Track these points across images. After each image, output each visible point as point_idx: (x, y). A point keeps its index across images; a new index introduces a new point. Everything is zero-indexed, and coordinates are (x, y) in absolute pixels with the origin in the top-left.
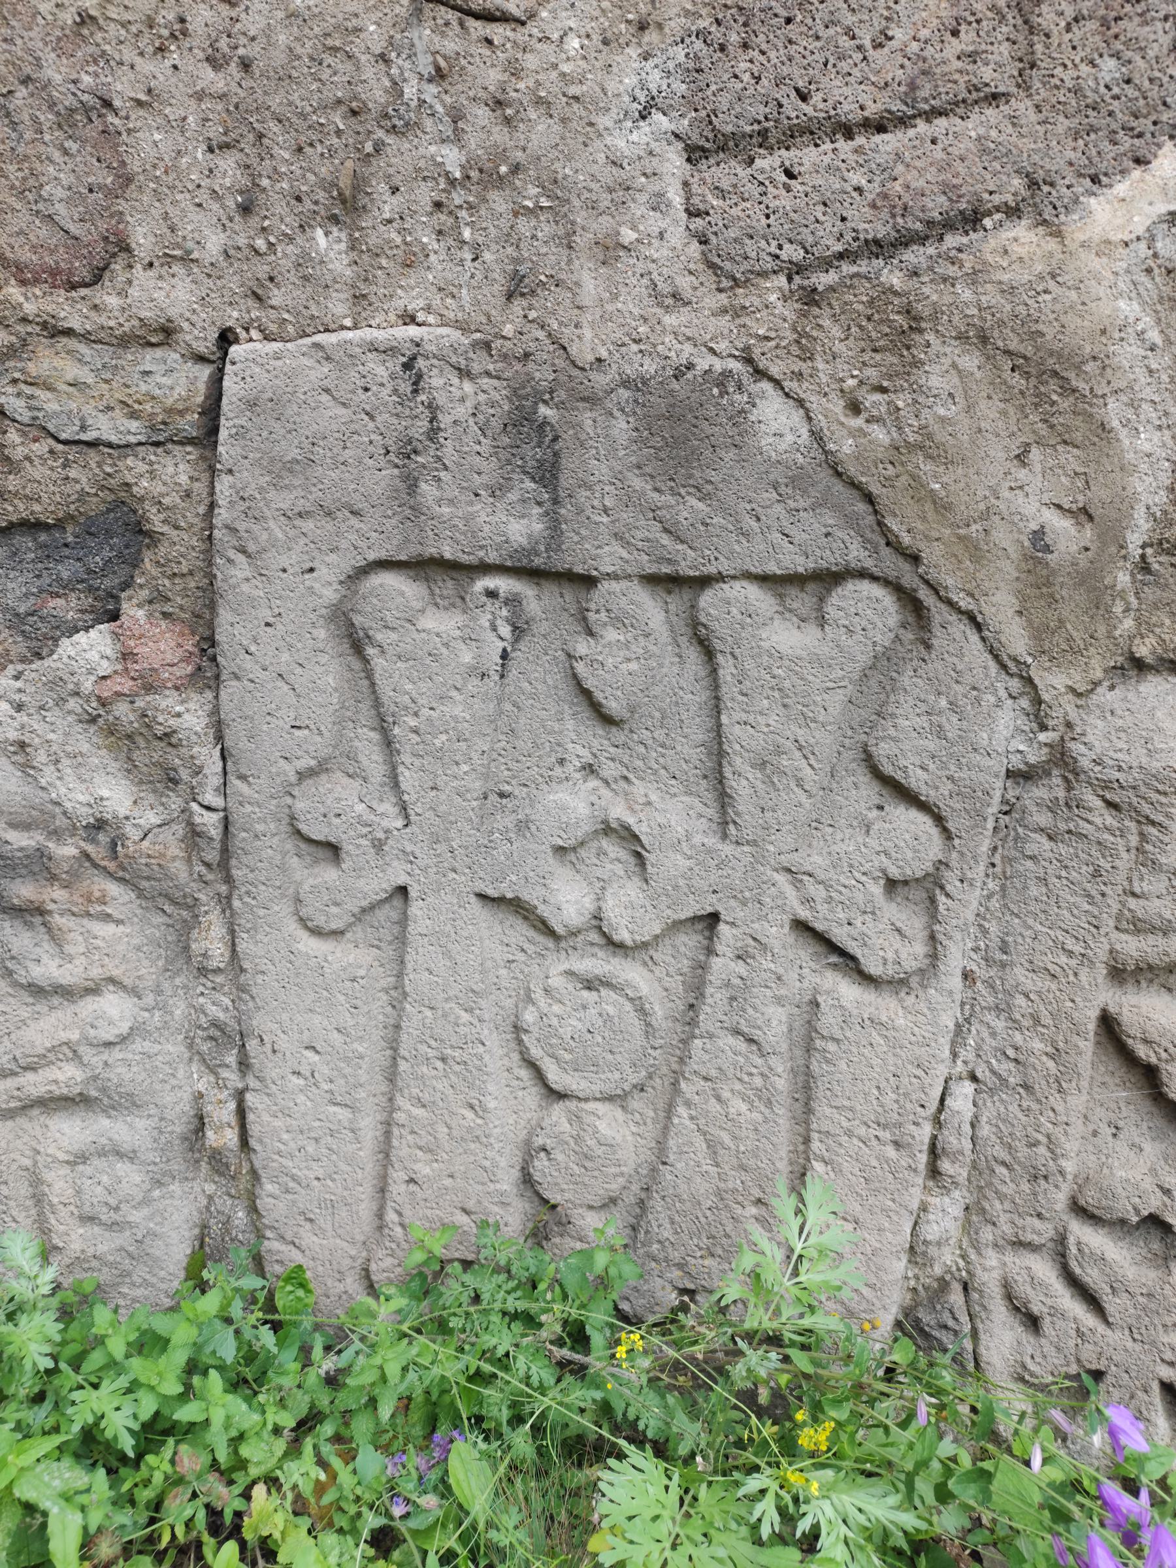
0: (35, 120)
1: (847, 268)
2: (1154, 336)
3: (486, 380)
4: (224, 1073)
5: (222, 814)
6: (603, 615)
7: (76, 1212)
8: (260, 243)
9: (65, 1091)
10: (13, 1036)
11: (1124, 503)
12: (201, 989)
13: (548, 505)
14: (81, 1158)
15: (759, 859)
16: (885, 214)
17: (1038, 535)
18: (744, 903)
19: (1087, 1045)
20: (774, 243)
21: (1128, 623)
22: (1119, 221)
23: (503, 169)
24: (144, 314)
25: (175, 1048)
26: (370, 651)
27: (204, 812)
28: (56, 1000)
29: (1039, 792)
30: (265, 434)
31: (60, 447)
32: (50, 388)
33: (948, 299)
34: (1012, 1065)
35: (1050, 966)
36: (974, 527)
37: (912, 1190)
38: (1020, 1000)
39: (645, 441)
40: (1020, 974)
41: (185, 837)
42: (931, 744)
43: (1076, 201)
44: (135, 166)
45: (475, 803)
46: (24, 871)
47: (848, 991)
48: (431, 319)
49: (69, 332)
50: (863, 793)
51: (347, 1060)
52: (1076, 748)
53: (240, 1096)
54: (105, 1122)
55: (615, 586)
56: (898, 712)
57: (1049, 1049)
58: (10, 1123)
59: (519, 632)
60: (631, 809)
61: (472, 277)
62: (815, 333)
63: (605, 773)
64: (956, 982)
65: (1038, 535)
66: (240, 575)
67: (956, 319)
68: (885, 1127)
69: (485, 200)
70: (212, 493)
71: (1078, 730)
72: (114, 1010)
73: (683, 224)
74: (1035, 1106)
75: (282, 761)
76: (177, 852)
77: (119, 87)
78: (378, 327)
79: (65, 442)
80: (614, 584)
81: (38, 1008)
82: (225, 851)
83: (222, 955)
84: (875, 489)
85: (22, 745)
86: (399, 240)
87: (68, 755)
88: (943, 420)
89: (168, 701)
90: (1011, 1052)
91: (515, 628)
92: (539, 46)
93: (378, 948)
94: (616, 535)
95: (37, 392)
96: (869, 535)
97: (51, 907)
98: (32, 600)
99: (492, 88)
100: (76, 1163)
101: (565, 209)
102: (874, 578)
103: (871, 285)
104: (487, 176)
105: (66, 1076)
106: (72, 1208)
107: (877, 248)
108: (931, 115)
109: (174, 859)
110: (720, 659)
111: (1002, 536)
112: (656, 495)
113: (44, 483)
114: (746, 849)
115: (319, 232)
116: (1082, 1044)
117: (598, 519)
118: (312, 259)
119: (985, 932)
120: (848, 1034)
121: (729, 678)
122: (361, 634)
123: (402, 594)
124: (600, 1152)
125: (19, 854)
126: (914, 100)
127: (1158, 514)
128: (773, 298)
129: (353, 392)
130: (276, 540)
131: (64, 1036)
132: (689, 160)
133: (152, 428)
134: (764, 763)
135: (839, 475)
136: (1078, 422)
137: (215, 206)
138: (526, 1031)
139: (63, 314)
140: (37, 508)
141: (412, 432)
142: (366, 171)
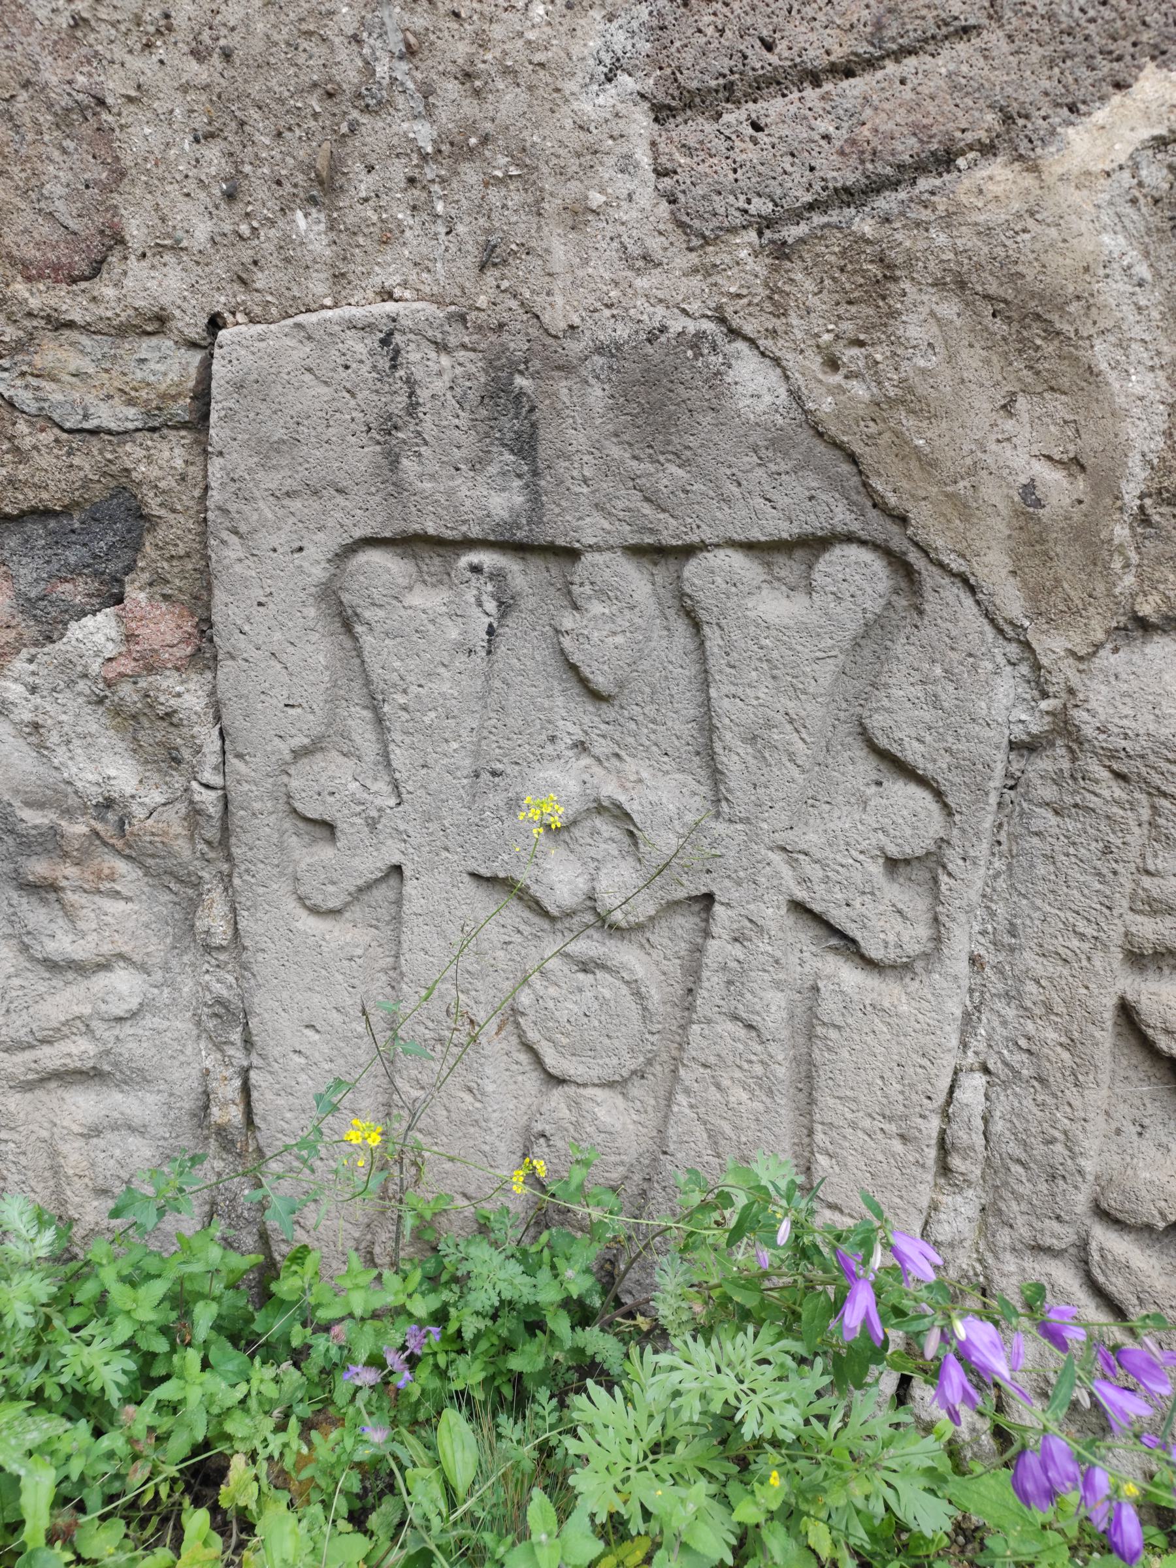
0: (35, 121)
1: (818, 219)
2: (1143, 270)
3: (463, 353)
4: (230, 1051)
5: (220, 792)
6: (587, 588)
7: (90, 1184)
8: (244, 229)
9: (78, 1064)
10: (31, 1010)
11: (1118, 450)
12: (206, 966)
13: (527, 477)
14: (93, 1132)
15: (753, 837)
16: (853, 161)
17: (1029, 489)
18: (739, 884)
19: (1105, 1037)
20: (742, 198)
21: (1129, 580)
22: (1099, 150)
23: (473, 141)
24: (139, 303)
25: (183, 1024)
26: (359, 629)
27: (203, 790)
28: (70, 976)
29: (1042, 764)
30: (252, 415)
31: (65, 436)
32: (54, 379)
33: (922, 245)
34: (1025, 1056)
35: (1061, 950)
36: (961, 484)
37: (921, 1187)
38: (1031, 987)
39: (620, 408)
40: (1028, 958)
41: (188, 815)
42: (928, 715)
43: (1053, 132)
44: (127, 161)
45: (465, 781)
46: (39, 849)
47: (850, 976)
48: (407, 294)
49: (70, 325)
50: (860, 768)
51: (346, 1039)
52: (1079, 715)
53: (245, 1073)
54: (119, 1097)
55: (598, 558)
56: (891, 681)
57: (1064, 1040)
58: (29, 1096)
59: (505, 607)
60: (622, 786)
61: (446, 250)
62: (787, 288)
63: (597, 751)
64: (962, 967)
65: (1029, 489)
66: (233, 555)
67: (931, 265)
68: (890, 1119)
69: (456, 173)
70: (205, 477)
71: (1081, 696)
72: (124, 985)
73: (651, 184)
74: (1050, 1100)
75: (277, 740)
76: (180, 830)
77: (111, 85)
78: (357, 304)
79: (70, 431)
80: (597, 556)
81: (54, 983)
82: (225, 830)
83: (224, 933)
84: (858, 448)
85: (36, 726)
86: (375, 218)
87: (78, 736)
88: (923, 371)
89: (169, 681)
90: (1023, 1042)
91: (501, 603)
92: (505, 15)
93: (377, 928)
94: (596, 505)
95: (43, 384)
96: (855, 497)
97: (64, 883)
98: (43, 585)
99: (460, 61)
100: (90, 1137)
101: (534, 176)
102: (863, 543)
103: (845, 234)
104: (458, 149)
105: (78, 1050)
106: (86, 1180)
107: (847, 196)
109: (177, 836)
110: (707, 630)
111: (992, 493)
112: (635, 463)
113: (52, 472)
114: (739, 827)
115: (299, 214)
116: (1098, 1034)
117: (578, 489)
118: (292, 241)
119: (993, 914)
120: (850, 1021)
121: (716, 650)
122: (350, 612)
123: (388, 571)
124: (599, 1140)
125: (34, 832)
126: (881, 40)
127: (1156, 461)
128: (743, 254)
129: (334, 370)
130: (266, 520)
131: (77, 1010)
132: (656, 120)
133: (148, 413)
134: (755, 737)
135: (820, 435)
136: (1064, 366)
137: (202, 195)
138: (523, 1014)
139: (64, 307)
140: (45, 495)
141: (392, 408)
142: (342, 152)
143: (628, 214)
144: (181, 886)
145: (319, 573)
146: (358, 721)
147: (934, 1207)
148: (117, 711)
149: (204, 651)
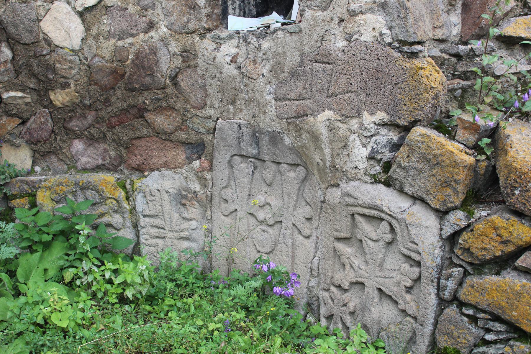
1: (293, 120)
11: (325, 160)
42: (310, 195)
44: (208, 94)
47: (301, 238)
50: (304, 203)
55: (268, 162)
59: (255, 168)
64: (315, 238)
65: (318, 162)
72: (194, 224)
82: (211, 199)
89: (206, 173)
104: (251, 100)
105: (185, 234)
108: (303, 100)
111: (315, 163)
113: (194, 138)
143: (271, 113)
144: (204, 207)
145: (228, 159)
146: (232, 183)
147: (310, 280)
148: (198, 177)
149: (211, 169)
